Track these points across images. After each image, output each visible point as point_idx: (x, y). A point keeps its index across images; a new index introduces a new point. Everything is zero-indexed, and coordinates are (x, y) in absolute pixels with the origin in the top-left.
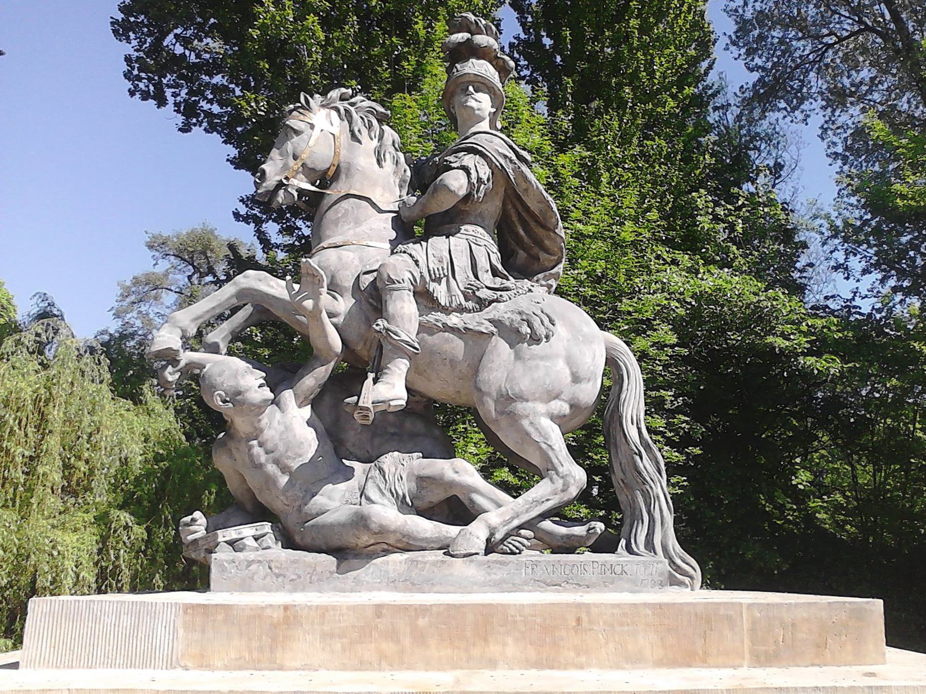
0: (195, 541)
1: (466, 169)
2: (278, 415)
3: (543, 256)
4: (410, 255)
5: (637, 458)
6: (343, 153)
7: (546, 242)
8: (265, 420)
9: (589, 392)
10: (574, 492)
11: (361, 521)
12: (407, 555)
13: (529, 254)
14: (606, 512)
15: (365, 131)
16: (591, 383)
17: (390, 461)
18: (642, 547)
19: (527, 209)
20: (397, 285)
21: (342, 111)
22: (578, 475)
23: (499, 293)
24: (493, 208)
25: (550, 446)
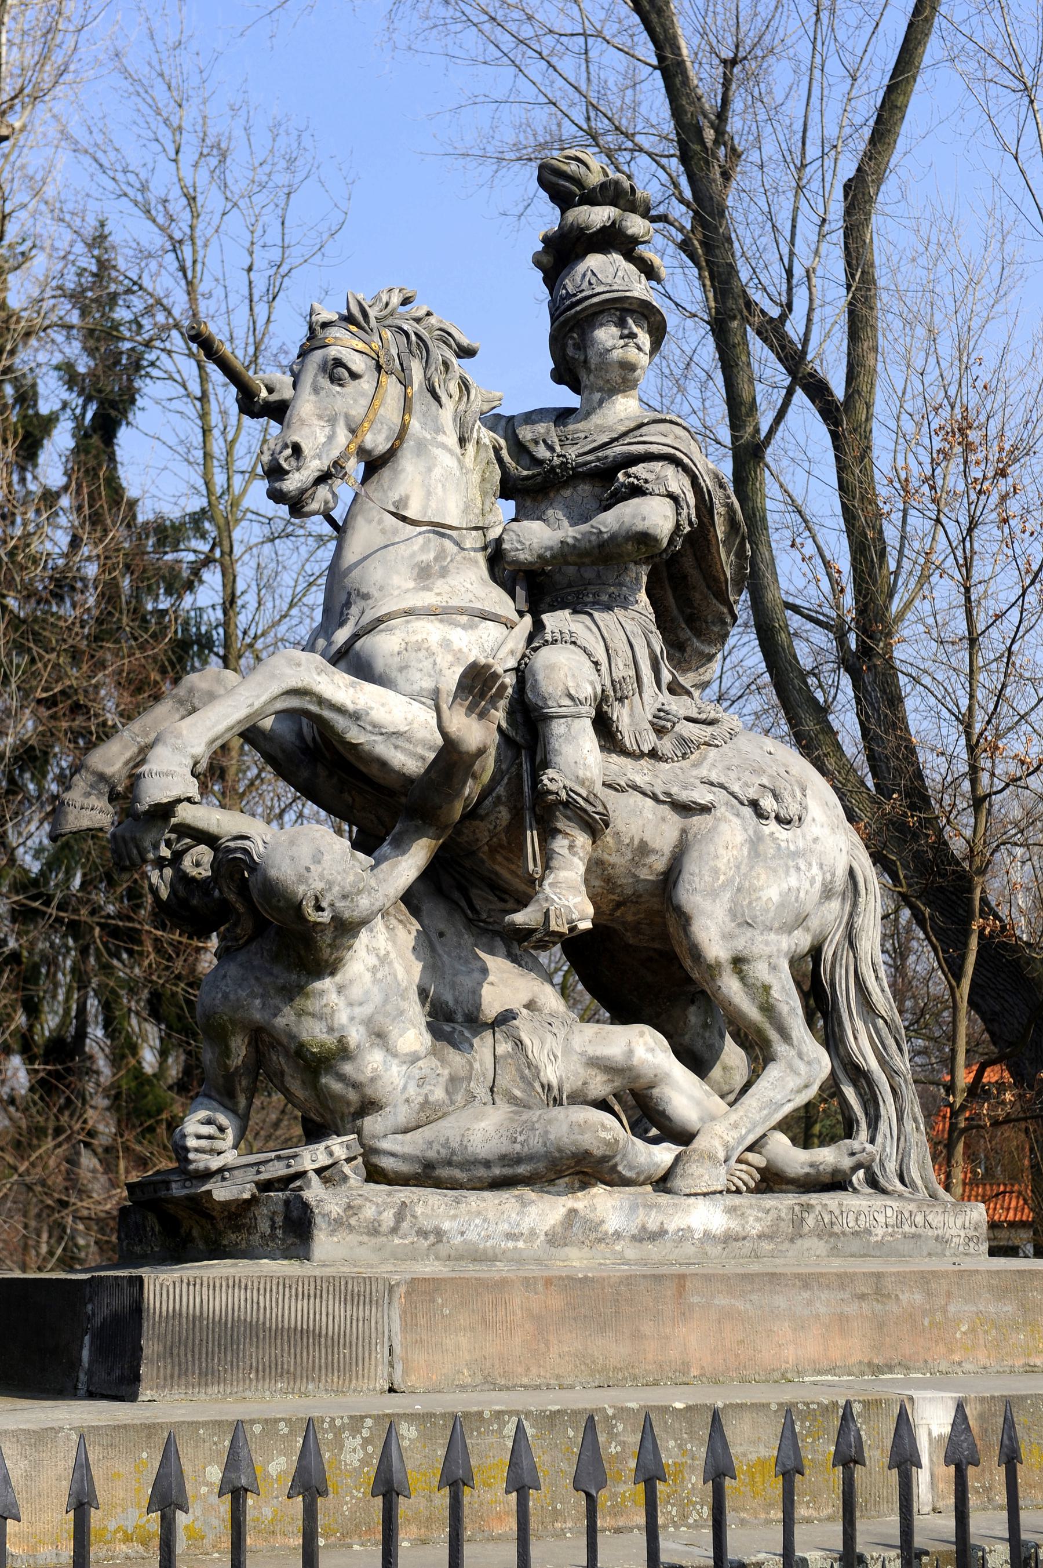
6: (415, 425)
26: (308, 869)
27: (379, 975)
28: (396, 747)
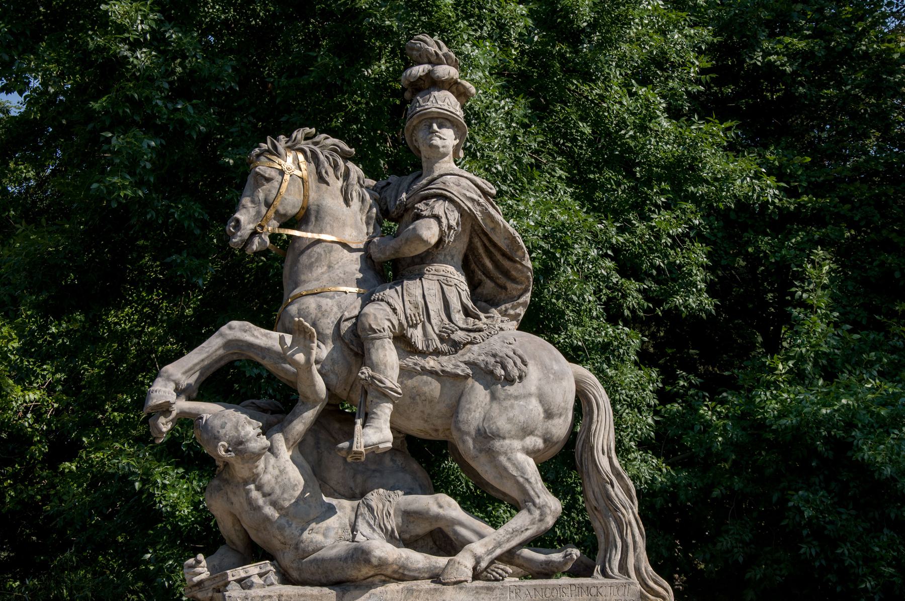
0: (201, 583)
1: (437, 218)
2: (272, 460)
3: (510, 285)
4: (388, 303)
5: (609, 487)
6: (313, 196)
7: (513, 273)
8: (261, 464)
9: (560, 427)
10: (550, 521)
11: (360, 555)
12: (402, 585)
13: (496, 283)
14: (579, 540)
15: (331, 171)
16: (562, 418)
17: (375, 497)
18: (616, 570)
19: (495, 245)
20: (379, 334)
21: (309, 153)
22: (554, 505)
23: (472, 334)
24: (461, 247)
25: (527, 480)
27: (279, 480)
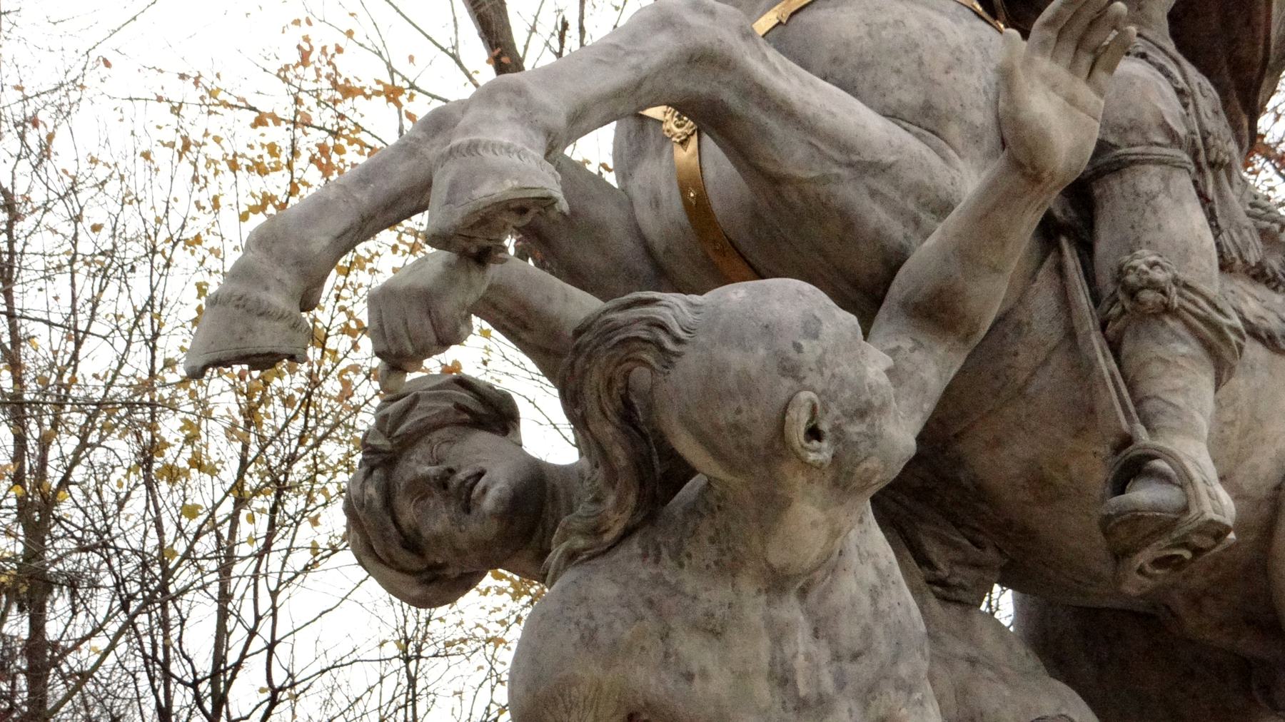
26: (798, 348)
27: (883, 605)
28: (873, 194)
